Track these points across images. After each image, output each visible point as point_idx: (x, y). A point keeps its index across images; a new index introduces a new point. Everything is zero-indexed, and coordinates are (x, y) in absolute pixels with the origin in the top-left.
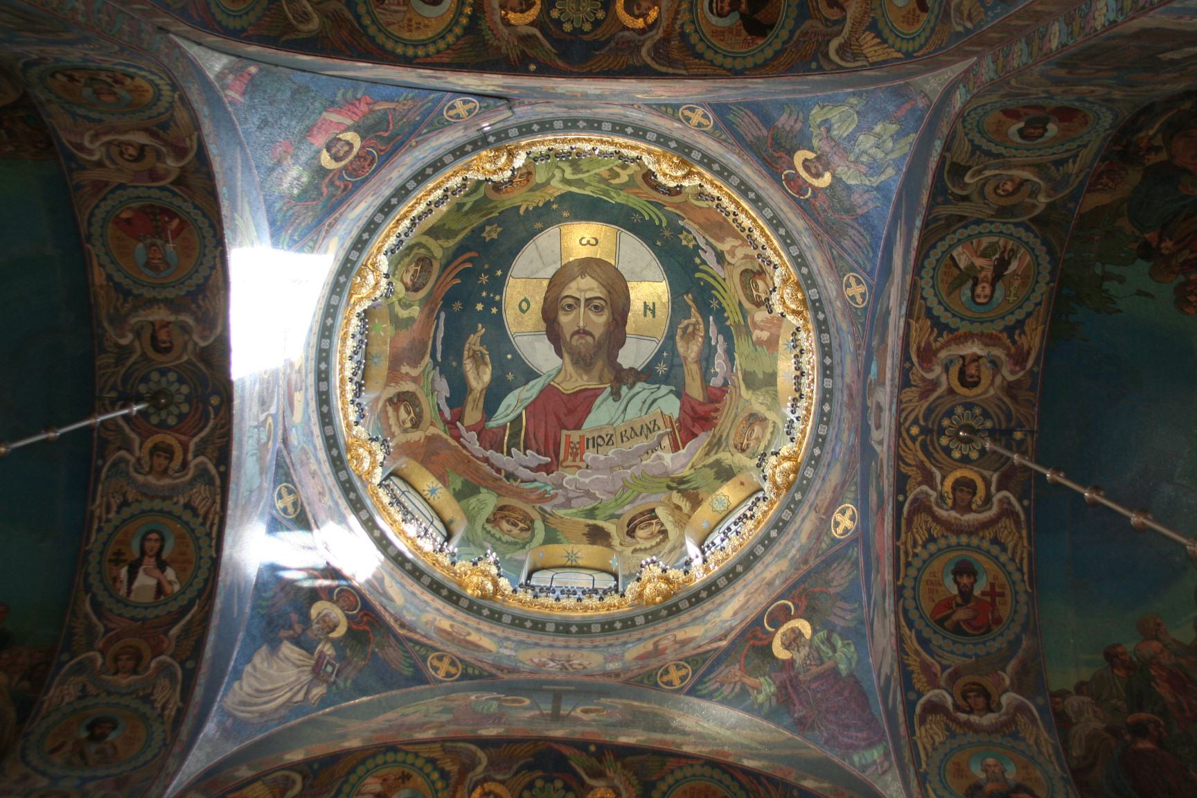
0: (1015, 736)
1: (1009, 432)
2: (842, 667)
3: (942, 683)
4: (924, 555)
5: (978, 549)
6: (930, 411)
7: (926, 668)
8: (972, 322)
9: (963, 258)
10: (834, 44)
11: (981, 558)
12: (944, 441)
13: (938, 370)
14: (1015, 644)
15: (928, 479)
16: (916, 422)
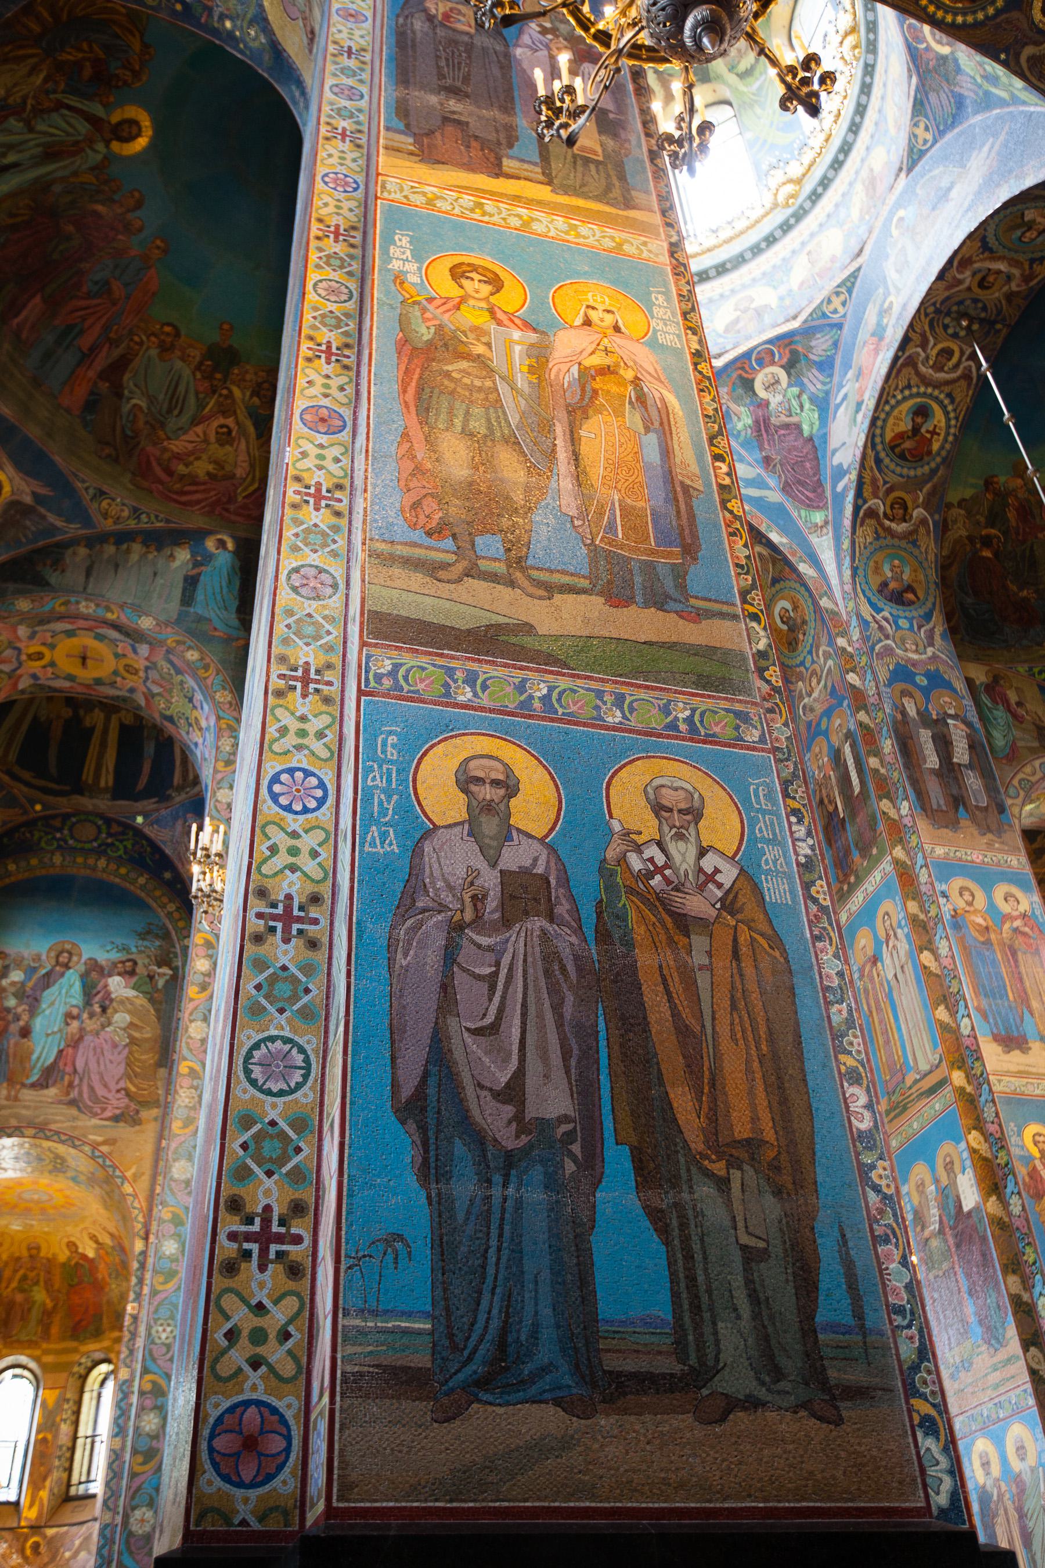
0: (914, 543)
1: (993, 323)
2: (806, 428)
3: (881, 495)
4: (899, 397)
5: (936, 399)
6: (948, 298)
7: (874, 481)
8: (1010, 250)
9: (1029, 215)
10: (1029, 51)
11: (935, 406)
12: (947, 321)
13: (968, 273)
14: (934, 472)
15: (924, 345)
16: (934, 304)
